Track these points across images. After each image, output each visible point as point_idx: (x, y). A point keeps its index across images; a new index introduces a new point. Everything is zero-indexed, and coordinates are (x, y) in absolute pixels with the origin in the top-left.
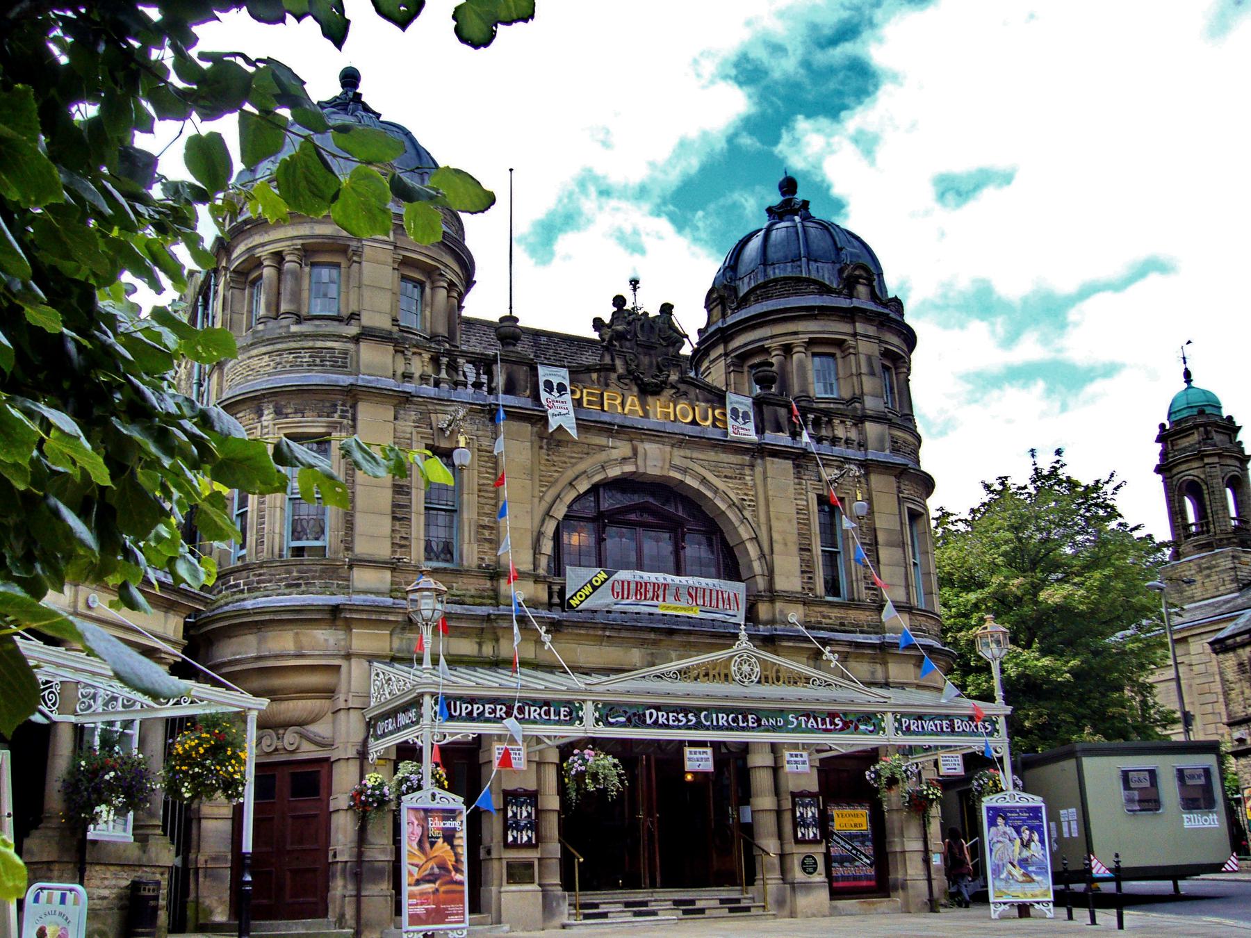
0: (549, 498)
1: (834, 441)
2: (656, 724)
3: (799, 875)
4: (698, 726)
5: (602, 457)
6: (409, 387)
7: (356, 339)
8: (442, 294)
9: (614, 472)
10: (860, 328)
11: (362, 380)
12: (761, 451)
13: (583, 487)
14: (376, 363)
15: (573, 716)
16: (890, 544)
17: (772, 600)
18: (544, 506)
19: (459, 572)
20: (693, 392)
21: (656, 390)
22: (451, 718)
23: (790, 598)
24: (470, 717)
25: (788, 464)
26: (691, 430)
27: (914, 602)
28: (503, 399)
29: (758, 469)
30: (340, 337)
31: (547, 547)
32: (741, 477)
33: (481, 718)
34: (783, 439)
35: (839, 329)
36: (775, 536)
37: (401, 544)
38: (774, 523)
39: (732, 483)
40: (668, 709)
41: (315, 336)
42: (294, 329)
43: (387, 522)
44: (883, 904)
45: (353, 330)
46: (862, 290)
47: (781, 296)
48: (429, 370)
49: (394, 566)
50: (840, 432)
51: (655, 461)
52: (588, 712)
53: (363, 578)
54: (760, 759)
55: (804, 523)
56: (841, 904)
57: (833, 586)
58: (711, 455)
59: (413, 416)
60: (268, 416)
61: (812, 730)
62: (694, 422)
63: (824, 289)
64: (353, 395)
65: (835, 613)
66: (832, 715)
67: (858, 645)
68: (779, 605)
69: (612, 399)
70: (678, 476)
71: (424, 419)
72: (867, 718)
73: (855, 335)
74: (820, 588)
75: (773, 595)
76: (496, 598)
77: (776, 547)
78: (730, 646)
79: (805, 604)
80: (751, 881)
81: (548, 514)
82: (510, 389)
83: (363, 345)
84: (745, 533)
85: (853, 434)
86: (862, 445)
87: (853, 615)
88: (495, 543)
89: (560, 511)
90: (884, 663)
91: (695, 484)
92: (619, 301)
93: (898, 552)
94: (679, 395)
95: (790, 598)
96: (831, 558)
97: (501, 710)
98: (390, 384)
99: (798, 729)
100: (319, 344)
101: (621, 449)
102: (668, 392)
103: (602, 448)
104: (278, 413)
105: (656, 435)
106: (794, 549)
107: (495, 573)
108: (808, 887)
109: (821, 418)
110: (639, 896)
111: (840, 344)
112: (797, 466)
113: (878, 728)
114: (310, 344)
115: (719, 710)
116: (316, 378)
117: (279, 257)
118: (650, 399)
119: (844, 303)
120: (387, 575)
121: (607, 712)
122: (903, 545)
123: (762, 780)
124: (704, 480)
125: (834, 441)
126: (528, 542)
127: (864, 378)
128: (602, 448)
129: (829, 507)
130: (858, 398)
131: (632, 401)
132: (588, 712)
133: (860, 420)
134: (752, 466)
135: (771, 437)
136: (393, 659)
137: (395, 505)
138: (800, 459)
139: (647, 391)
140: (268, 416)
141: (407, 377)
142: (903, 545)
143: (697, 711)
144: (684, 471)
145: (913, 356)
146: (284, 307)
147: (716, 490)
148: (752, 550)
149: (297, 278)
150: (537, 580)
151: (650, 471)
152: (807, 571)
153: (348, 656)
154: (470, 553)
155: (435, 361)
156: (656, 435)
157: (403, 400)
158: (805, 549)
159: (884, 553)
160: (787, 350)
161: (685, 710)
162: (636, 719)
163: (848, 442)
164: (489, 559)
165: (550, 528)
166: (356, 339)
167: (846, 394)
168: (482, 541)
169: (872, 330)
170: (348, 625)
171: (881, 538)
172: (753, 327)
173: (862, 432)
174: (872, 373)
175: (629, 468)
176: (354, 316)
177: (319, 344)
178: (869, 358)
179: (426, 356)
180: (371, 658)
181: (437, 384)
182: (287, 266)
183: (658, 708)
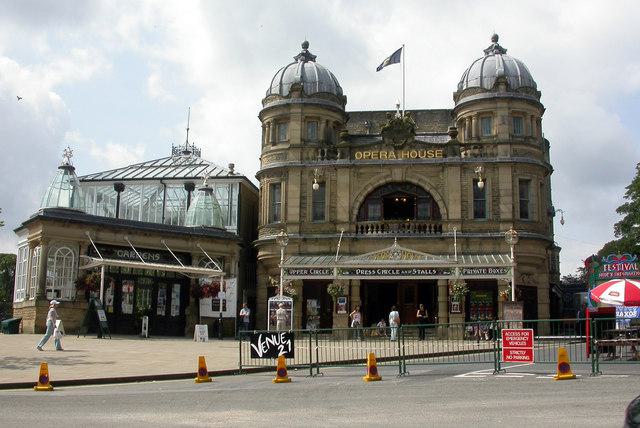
1: (486, 155)
4: (376, 274)
5: (377, 176)
8: (323, 126)
9: (382, 182)
10: (499, 105)
12: (444, 166)
13: (370, 189)
15: (330, 272)
21: (401, 148)
23: (455, 222)
31: (356, 212)
32: (438, 176)
40: (365, 269)
43: (298, 210)
46: (502, 87)
51: (398, 175)
61: (423, 275)
66: (432, 269)
67: (484, 238)
69: (383, 154)
72: (447, 270)
74: (471, 215)
76: (336, 231)
81: (356, 200)
84: (437, 198)
88: (336, 213)
89: (361, 199)
90: (499, 244)
95: (455, 222)
101: (386, 172)
102: (407, 147)
106: (459, 203)
107: (335, 222)
111: (492, 112)
118: (399, 151)
123: (441, 291)
125: (486, 155)
126: (347, 210)
131: (392, 153)
133: (495, 145)
139: (398, 149)
143: (376, 269)
148: (440, 204)
154: (327, 217)
155: (317, 150)
161: (371, 269)
165: (358, 205)
169: (505, 105)
171: (502, 193)
179: (313, 150)
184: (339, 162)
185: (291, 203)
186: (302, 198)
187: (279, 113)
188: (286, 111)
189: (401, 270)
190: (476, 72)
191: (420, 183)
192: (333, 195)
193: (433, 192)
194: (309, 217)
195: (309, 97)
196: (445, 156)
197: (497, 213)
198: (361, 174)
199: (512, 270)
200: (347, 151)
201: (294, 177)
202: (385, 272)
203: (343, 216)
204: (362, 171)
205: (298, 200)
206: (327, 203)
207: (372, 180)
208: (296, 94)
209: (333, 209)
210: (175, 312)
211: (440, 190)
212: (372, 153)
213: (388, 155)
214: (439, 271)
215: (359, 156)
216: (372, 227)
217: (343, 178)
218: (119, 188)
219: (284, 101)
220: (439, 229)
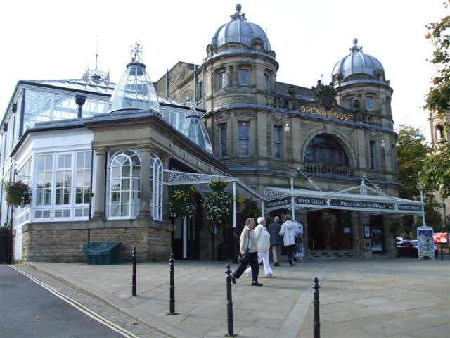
0: (304, 139)
1: (373, 124)
2: (343, 206)
3: (365, 247)
5: (316, 128)
6: (269, 108)
7: (256, 93)
9: (320, 133)
10: (381, 89)
11: (258, 105)
12: (357, 127)
14: (261, 100)
15: (325, 203)
16: (388, 155)
17: (359, 170)
18: (302, 143)
19: (283, 161)
20: (339, 109)
22: (298, 203)
23: (364, 170)
24: (302, 203)
25: (362, 131)
26: (338, 121)
27: (394, 172)
28: (293, 112)
29: (355, 133)
30: (251, 93)
33: (305, 203)
34: (361, 124)
35: (374, 89)
36: (360, 152)
37: (269, 153)
38: (360, 149)
39: (349, 136)
41: (245, 92)
42: (239, 90)
44: (384, 256)
45: (255, 91)
47: (358, 79)
48: (273, 102)
49: (268, 159)
50: (375, 121)
51: (330, 129)
52: (328, 202)
53: (262, 163)
54: (355, 215)
55: (366, 148)
56: (375, 256)
57: (373, 168)
58: (343, 128)
59: (270, 116)
60: (232, 115)
62: (339, 118)
63: (370, 77)
64: (256, 110)
65: (374, 174)
66: (383, 204)
68: (360, 172)
69: (319, 111)
70: (335, 134)
71: (273, 118)
73: (379, 92)
74: (370, 168)
75: (359, 169)
77: (360, 155)
78: (360, 185)
79: (367, 171)
80: (351, 248)
81: (304, 145)
82: (294, 109)
83: (258, 95)
85: (378, 122)
86: (381, 125)
87: (379, 175)
89: (307, 144)
91: (339, 136)
92: (319, 82)
93: (389, 157)
94: (335, 110)
95: (364, 170)
96: (372, 158)
97: (309, 201)
98: (265, 107)
99: (375, 208)
100: (246, 95)
101: (320, 126)
102: (333, 109)
103: (316, 126)
104: (235, 114)
105: (330, 122)
108: (367, 250)
109: (371, 116)
110: (325, 252)
111: (374, 94)
112: (365, 132)
113: (394, 208)
114: (242, 94)
115: (357, 202)
116: (245, 105)
117: (232, 67)
118: (328, 111)
119: (376, 82)
120: (267, 162)
121: (333, 201)
122: (391, 155)
124: (342, 136)
127: (382, 105)
128: (316, 126)
129: (372, 143)
130: (379, 111)
131: (323, 113)
132: (328, 202)
133: (381, 117)
134: (353, 131)
135: (358, 123)
136: (270, 186)
137: (268, 142)
138: (366, 129)
139: (327, 109)
140: (232, 115)
141: (268, 104)
142: (391, 155)
143: (352, 202)
144: (337, 132)
145: (392, 96)
146: (234, 83)
147: (345, 138)
149: (237, 73)
150: (303, 164)
151: (329, 133)
152: (367, 163)
153: (258, 185)
156: (330, 122)
157: (269, 111)
158: (367, 156)
159: (387, 157)
160: (360, 95)
161: (349, 202)
162: (339, 204)
163: (377, 124)
164: (290, 158)
166: (256, 93)
167: (376, 109)
168: (288, 152)
170: (258, 176)
172: (349, 88)
173: (381, 122)
174: (384, 103)
175: (323, 132)
176: (254, 86)
177: (246, 95)
178: (383, 99)
180: (264, 185)
181: (275, 107)
182: (234, 71)
183: (344, 201)
184: (293, 112)
185: (260, 141)
186: (268, 138)
187: (245, 60)
188: (251, 60)
189: (367, 203)
190: (347, 65)
191: (341, 138)
192: (290, 138)
193: (349, 146)
194: (273, 156)
195: (267, 52)
196: (354, 120)
197: (384, 167)
198: (306, 124)
199: (423, 208)
200: (297, 103)
201: (262, 119)
202: (358, 204)
203: (297, 157)
204: (306, 122)
205: (266, 139)
206: (285, 145)
207: (312, 131)
208: (258, 47)
209: (290, 150)
210: (194, 238)
211: (352, 145)
212: (312, 110)
213: (321, 113)
214: (388, 205)
215: (304, 110)
216: (315, 168)
217: (296, 124)
218: (80, 101)
219: (247, 51)
220: (352, 175)
